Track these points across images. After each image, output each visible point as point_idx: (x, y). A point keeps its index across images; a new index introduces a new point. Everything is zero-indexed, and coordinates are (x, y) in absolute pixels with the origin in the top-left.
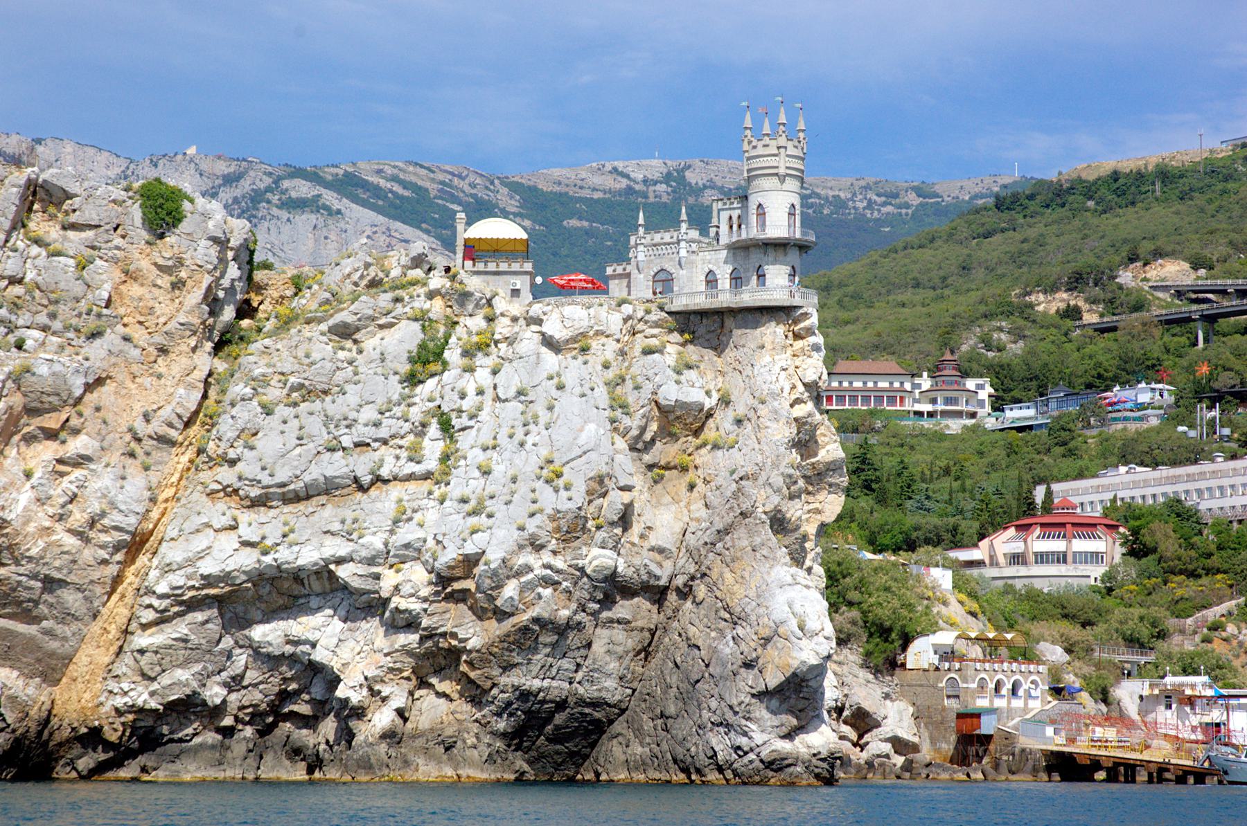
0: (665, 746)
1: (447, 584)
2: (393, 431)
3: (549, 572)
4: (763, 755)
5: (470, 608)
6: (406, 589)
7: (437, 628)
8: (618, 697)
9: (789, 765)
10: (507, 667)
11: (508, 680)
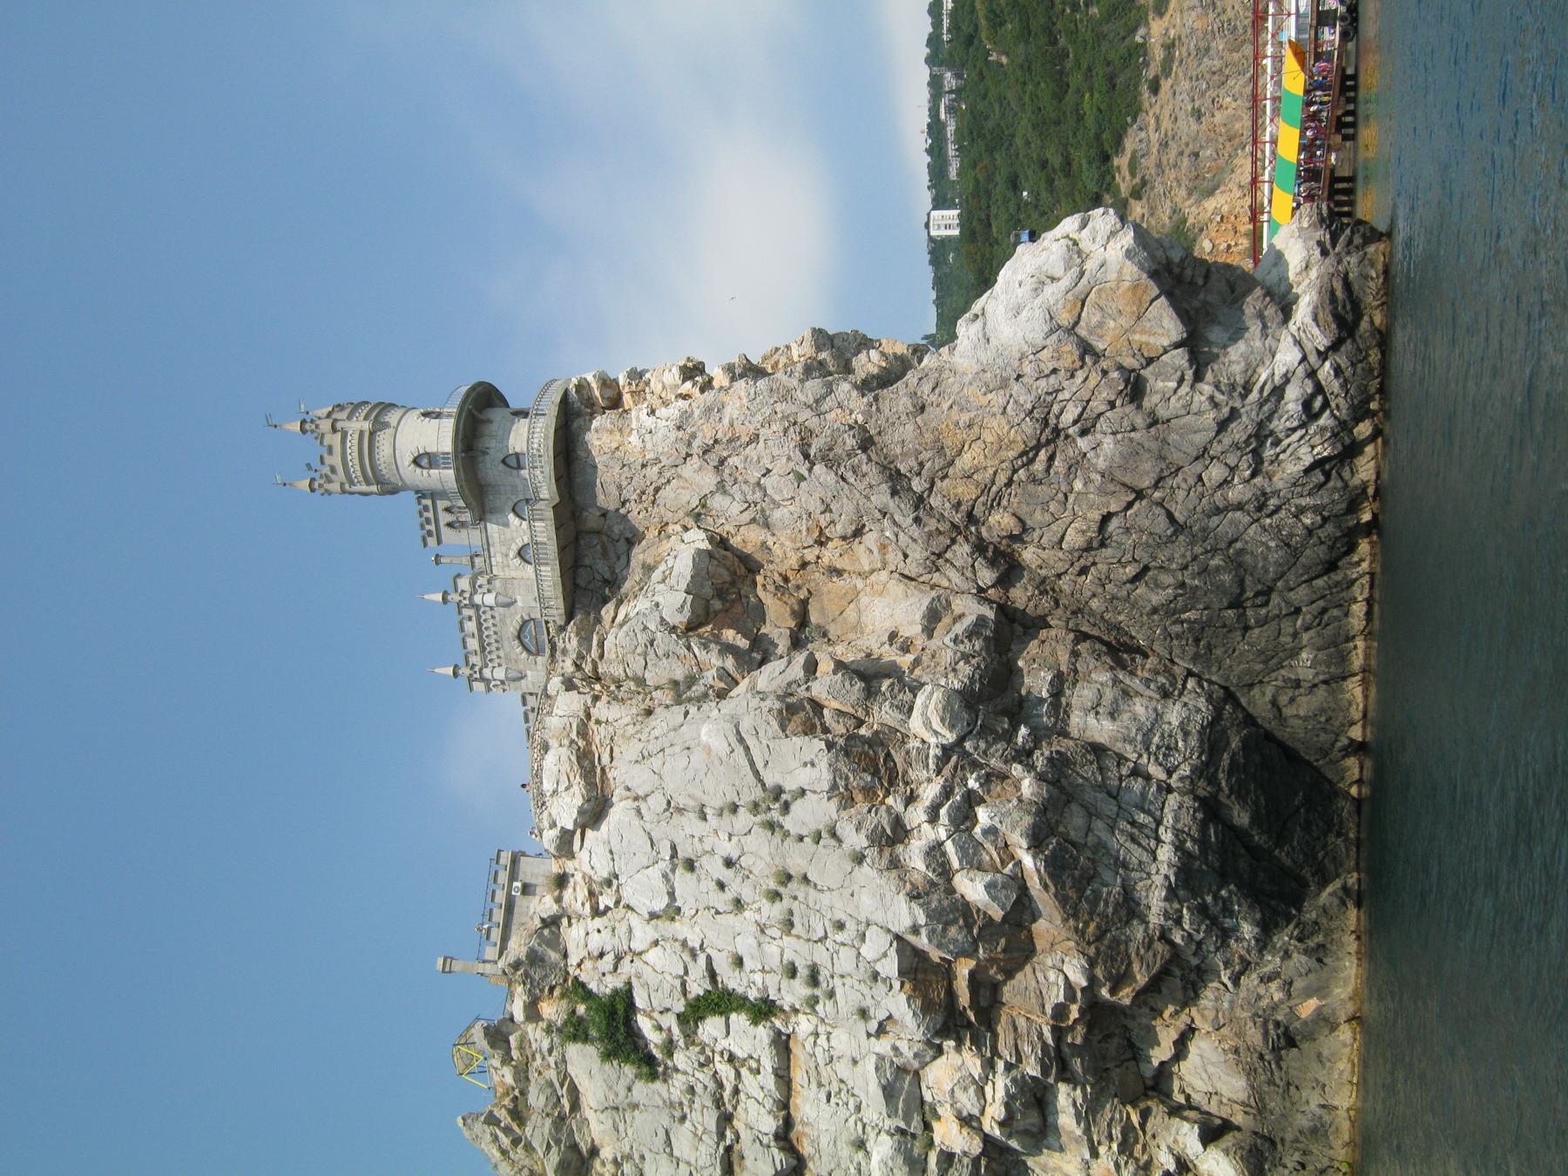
0: (1301, 594)
1: (962, 1014)
2: (709, 1103)
3: (943, 811)
4: (1321, 340)
5: (1010, 974)
6: (968, 1103)
7: (1045, 1045)
8: (1202, 703)
9: (1347, 285)
10: (1131, 908)
11: (1154, 910)
